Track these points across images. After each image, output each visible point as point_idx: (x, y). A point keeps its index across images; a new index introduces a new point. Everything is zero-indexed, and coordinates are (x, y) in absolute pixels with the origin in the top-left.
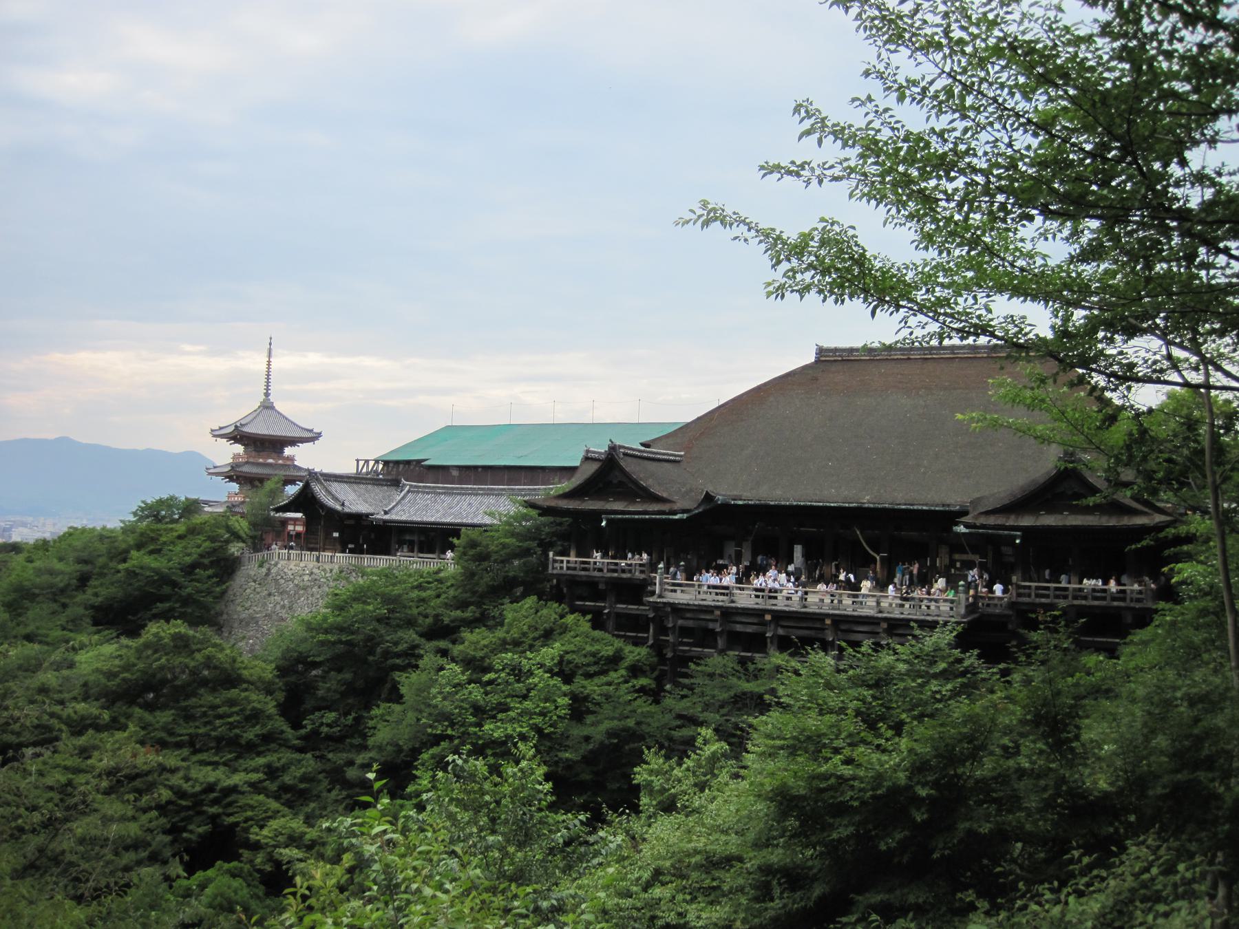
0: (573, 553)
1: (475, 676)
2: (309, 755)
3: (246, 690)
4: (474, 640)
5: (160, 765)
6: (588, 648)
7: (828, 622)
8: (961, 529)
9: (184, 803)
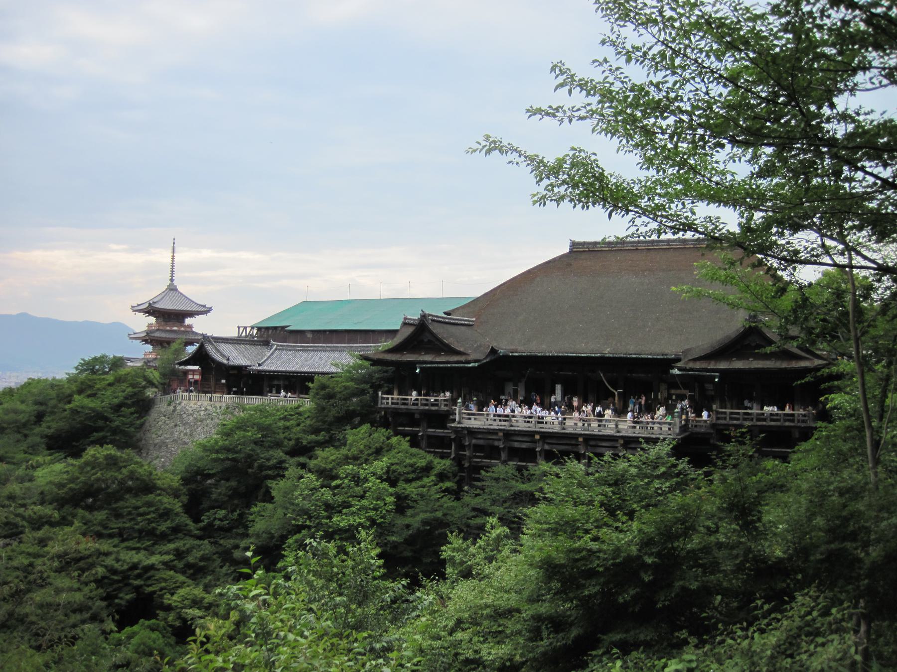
0: (396, 392)
1: (326, 482)
2: (206, 542)
3: (160, 495)
4: (325, 456)
5: (98, 550)
6: (408, 461)
7: (581, 439)
8: (676, 371)
9: (116, 578)
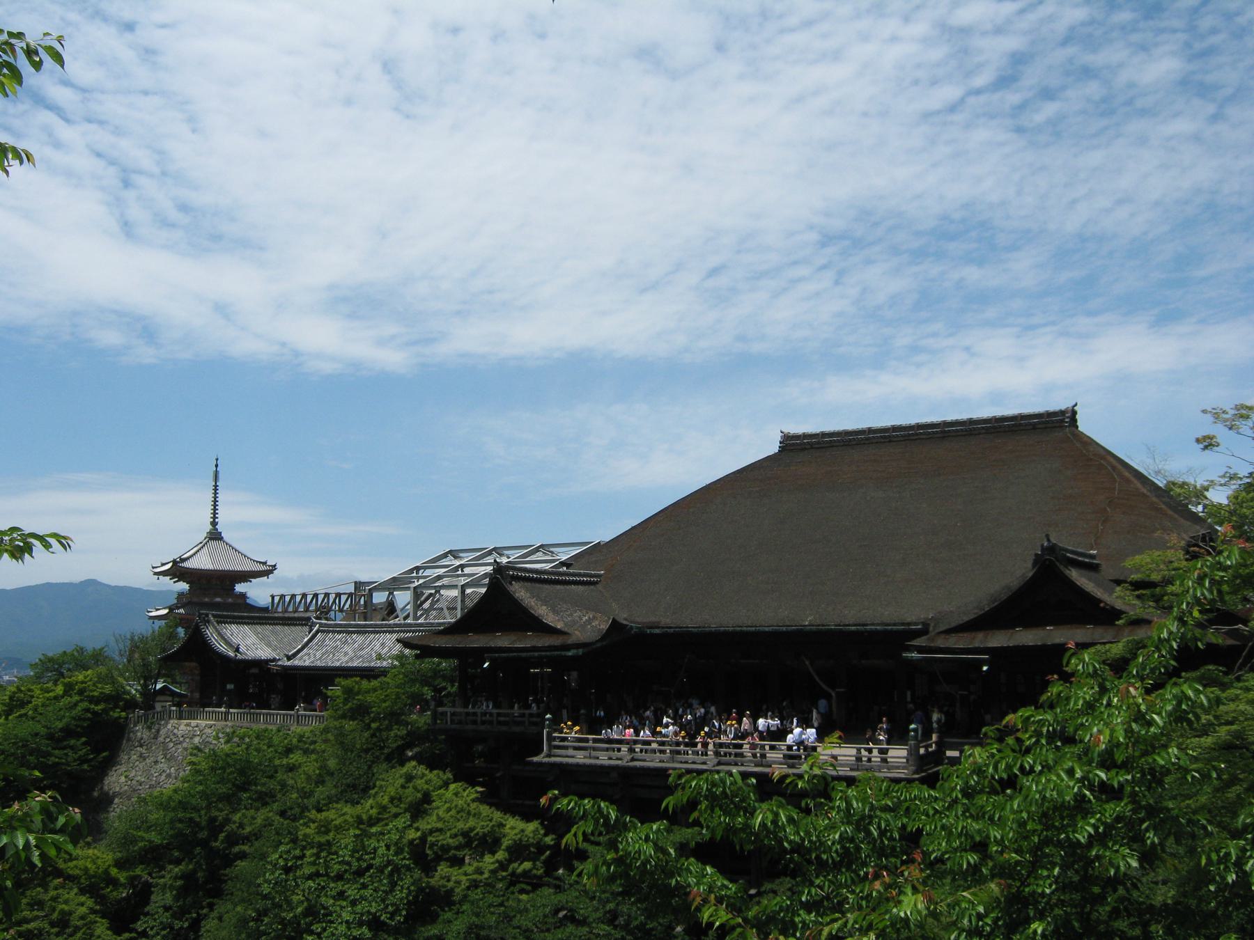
6: (460, 825)
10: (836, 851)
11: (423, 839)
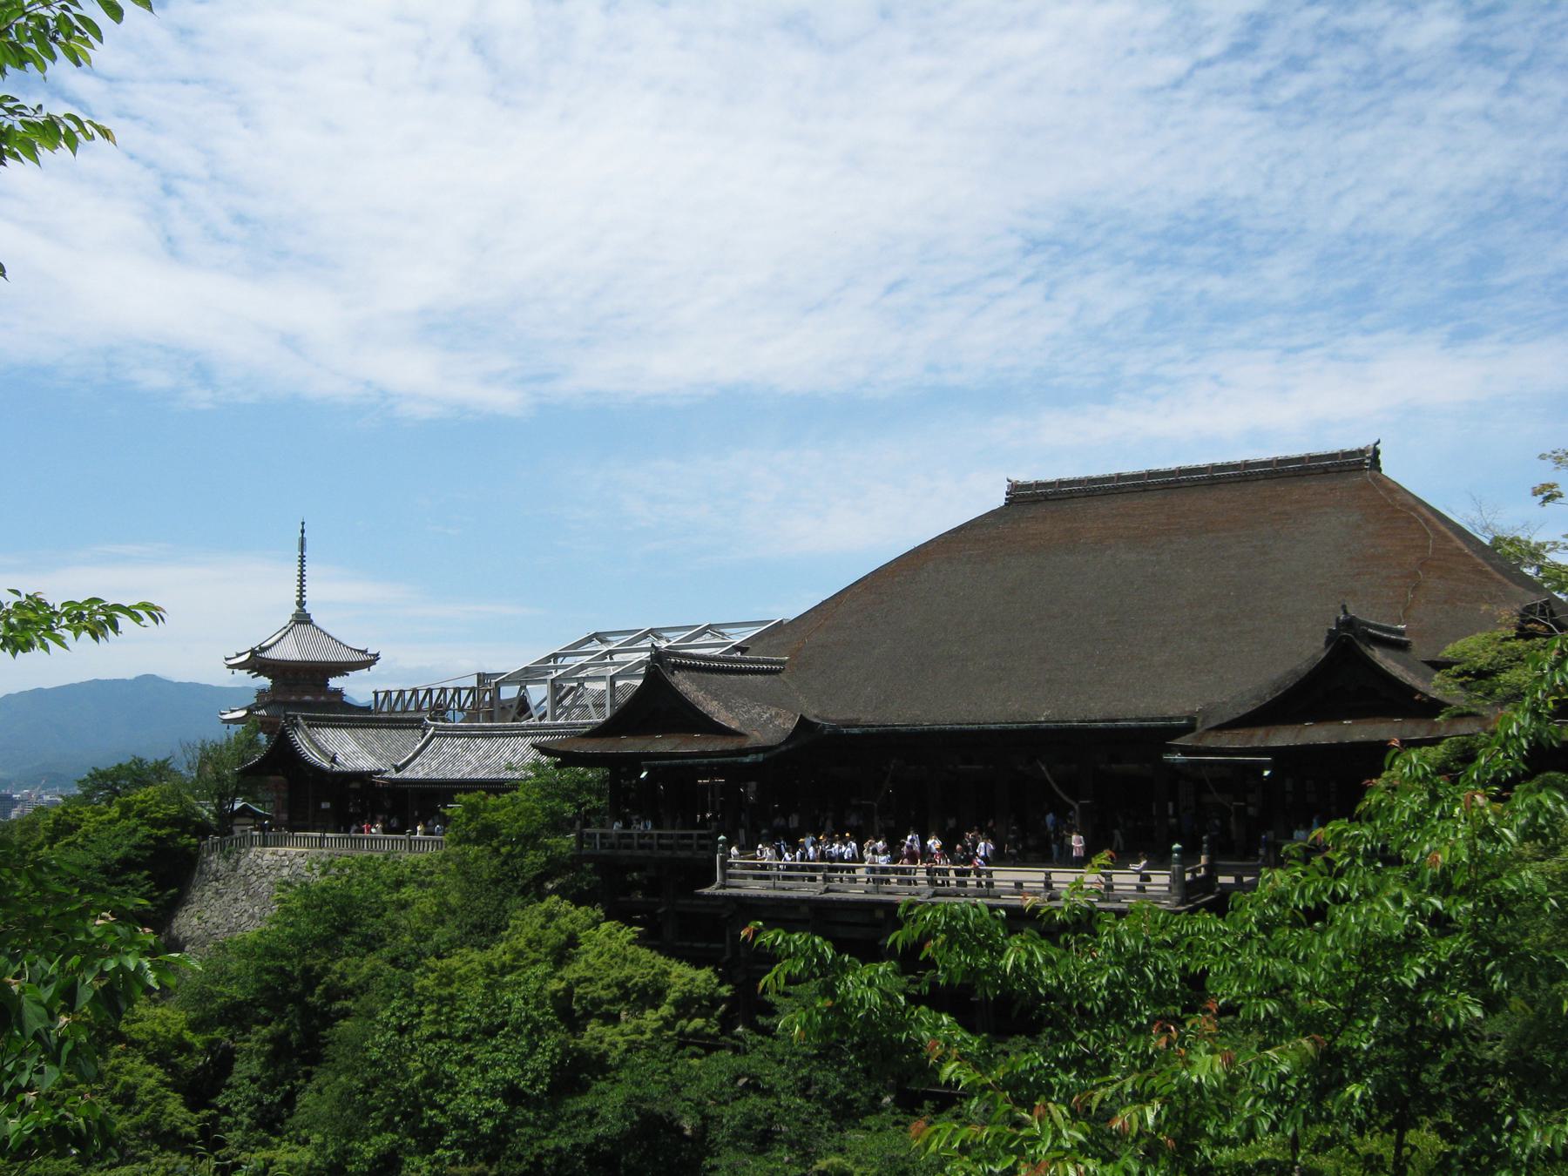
6: (614, 973)
10: (1103, 998)
11: (569, 991)
